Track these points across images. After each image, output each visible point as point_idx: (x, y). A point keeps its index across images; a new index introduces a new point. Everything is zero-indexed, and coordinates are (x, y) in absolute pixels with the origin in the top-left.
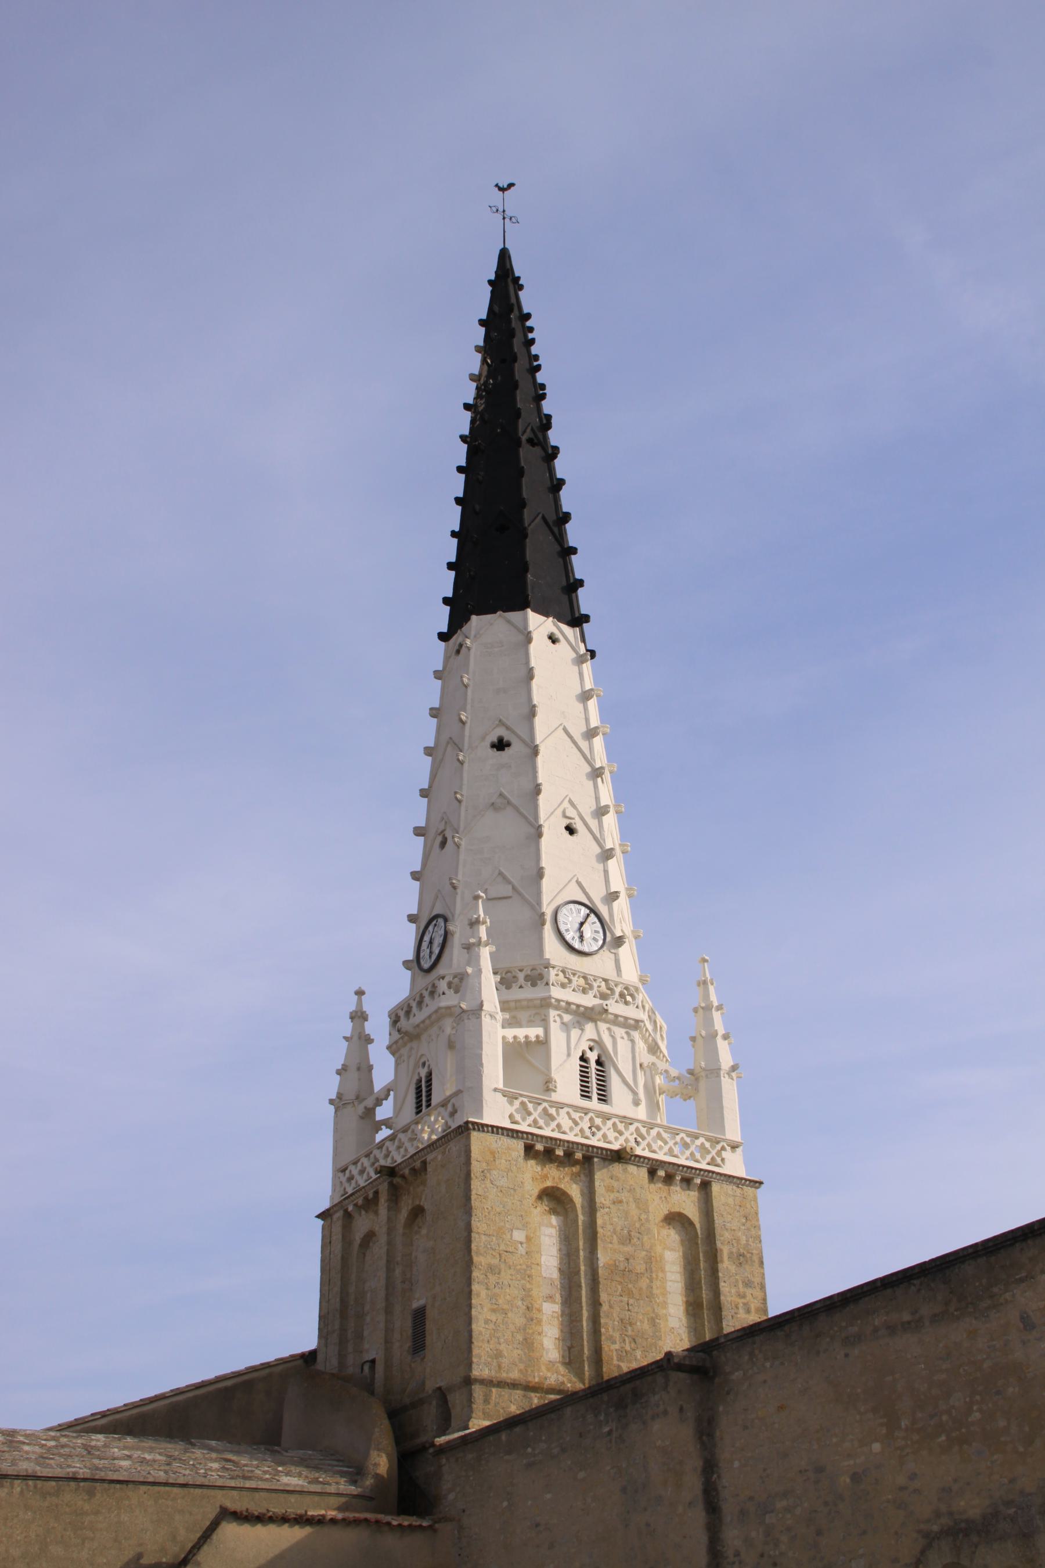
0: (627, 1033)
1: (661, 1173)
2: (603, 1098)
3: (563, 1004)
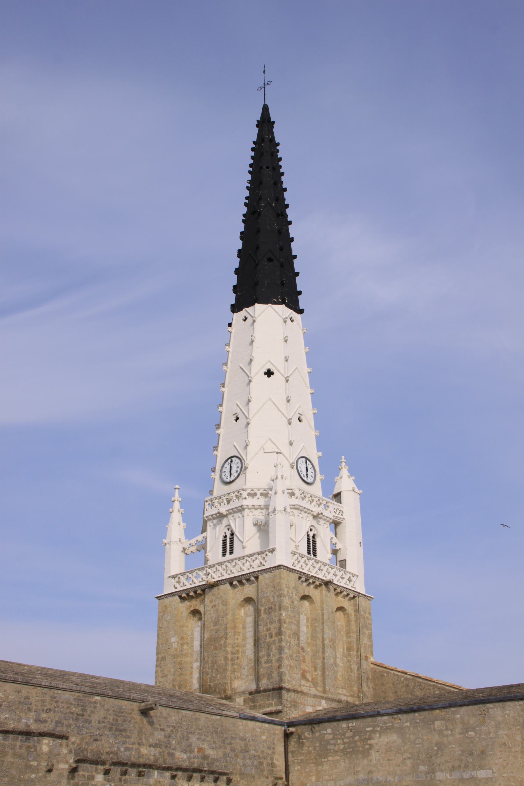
0: (241, 513)
1: (235, 583)
2: (231, 552)
3: (215, 516)
